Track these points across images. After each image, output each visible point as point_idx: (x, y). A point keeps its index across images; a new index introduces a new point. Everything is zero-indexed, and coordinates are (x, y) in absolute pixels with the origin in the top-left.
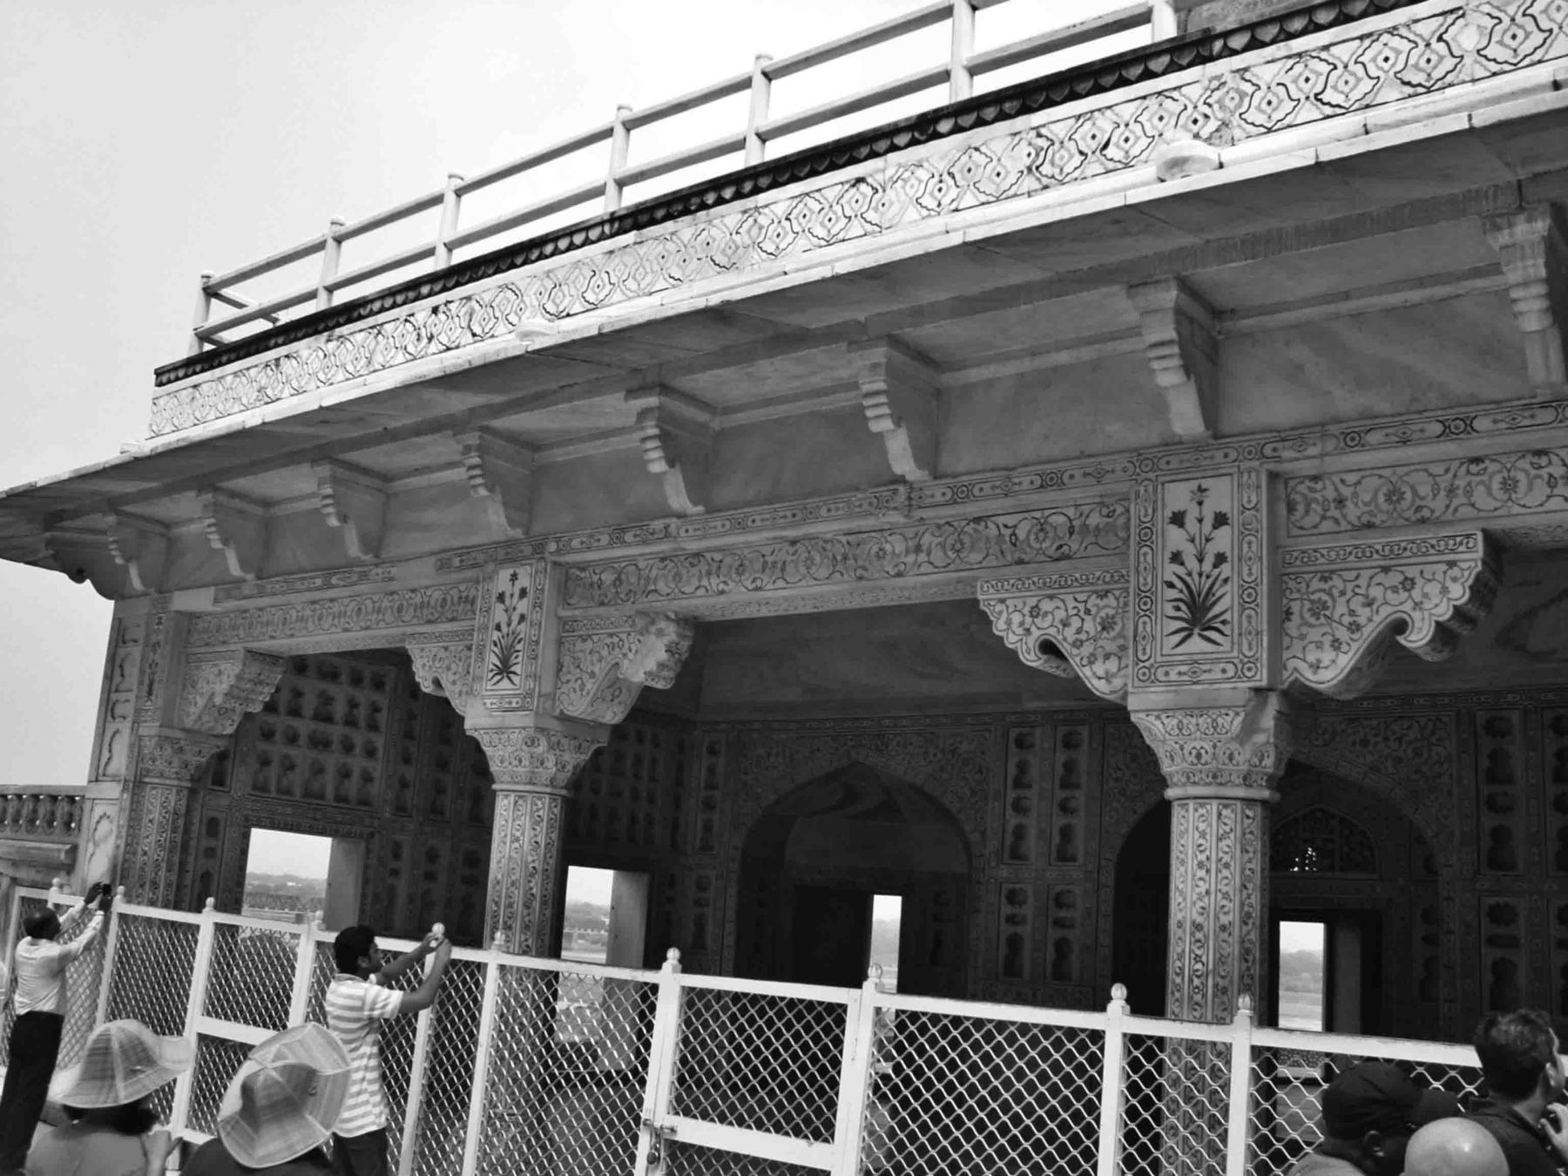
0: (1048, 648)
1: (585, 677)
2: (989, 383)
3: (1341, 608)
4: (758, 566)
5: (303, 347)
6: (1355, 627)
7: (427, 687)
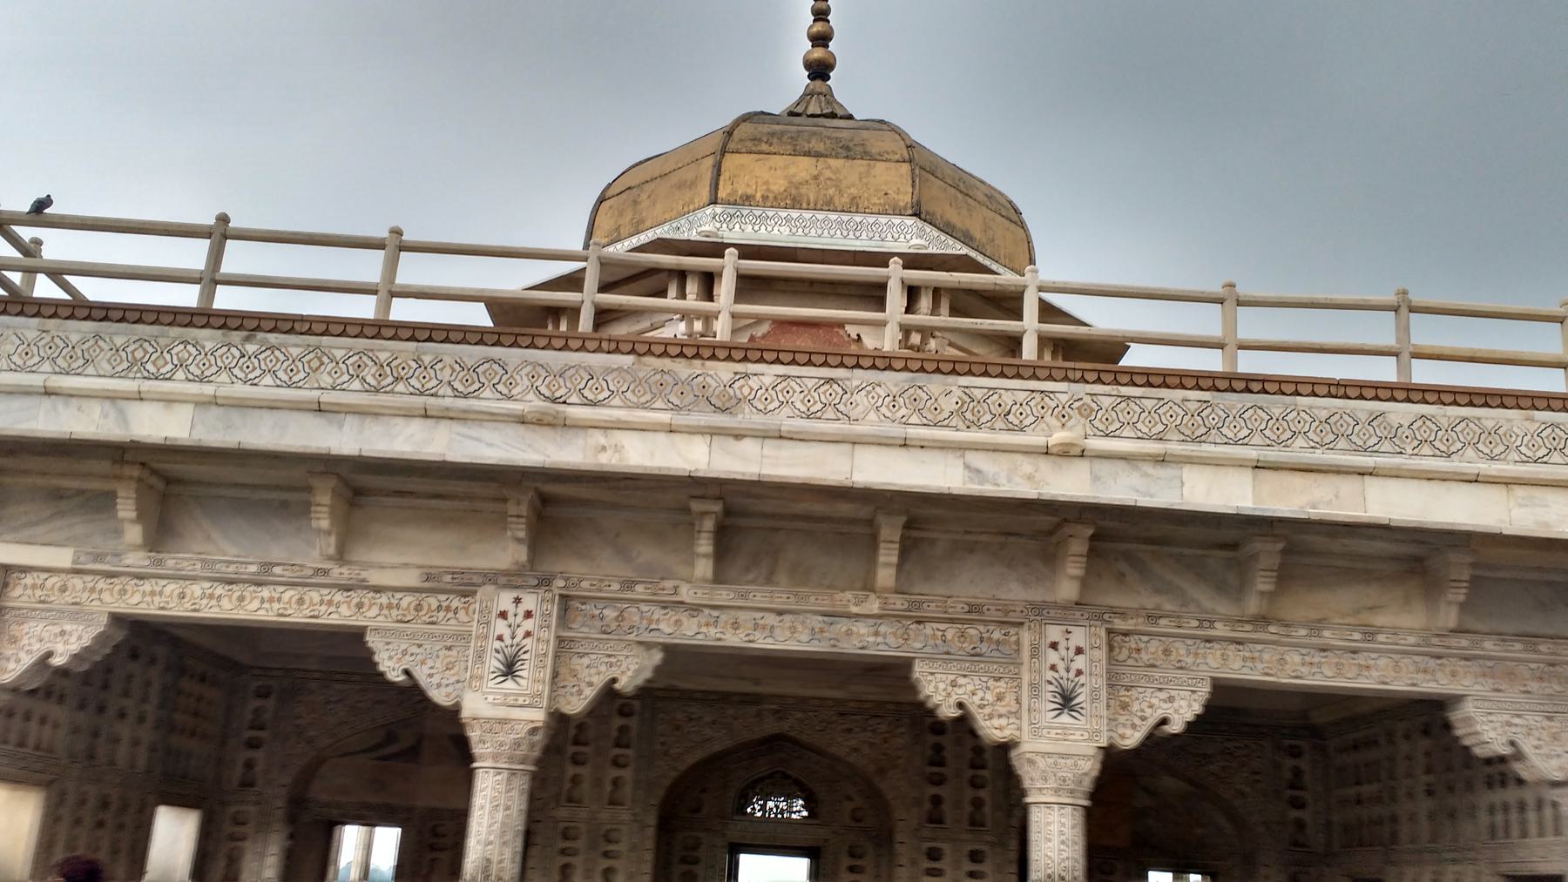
0: (960, 705)
1: (583, 685)
2: (932, 542)
3: (1136, 707)
4: (751, 625)
5: (208, 338)
6: (1143, 719)
7: (395, 676)
